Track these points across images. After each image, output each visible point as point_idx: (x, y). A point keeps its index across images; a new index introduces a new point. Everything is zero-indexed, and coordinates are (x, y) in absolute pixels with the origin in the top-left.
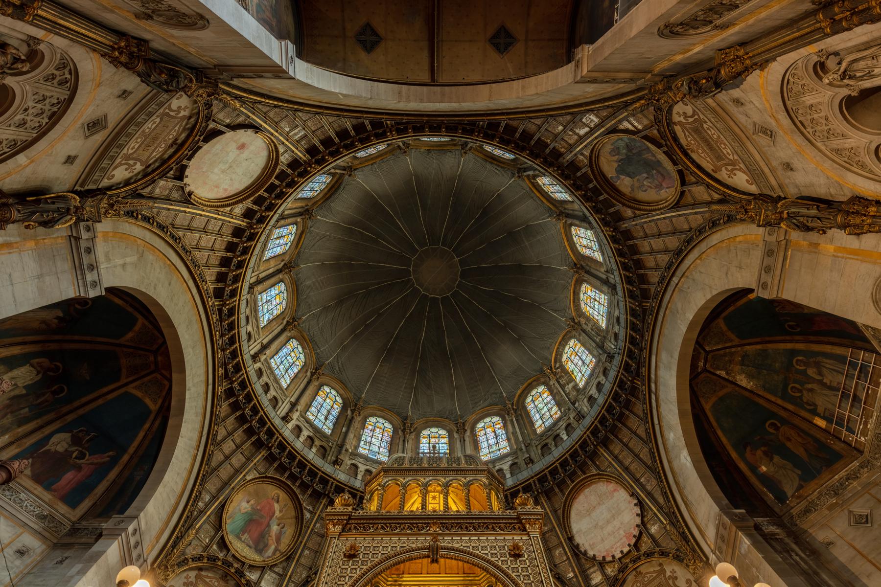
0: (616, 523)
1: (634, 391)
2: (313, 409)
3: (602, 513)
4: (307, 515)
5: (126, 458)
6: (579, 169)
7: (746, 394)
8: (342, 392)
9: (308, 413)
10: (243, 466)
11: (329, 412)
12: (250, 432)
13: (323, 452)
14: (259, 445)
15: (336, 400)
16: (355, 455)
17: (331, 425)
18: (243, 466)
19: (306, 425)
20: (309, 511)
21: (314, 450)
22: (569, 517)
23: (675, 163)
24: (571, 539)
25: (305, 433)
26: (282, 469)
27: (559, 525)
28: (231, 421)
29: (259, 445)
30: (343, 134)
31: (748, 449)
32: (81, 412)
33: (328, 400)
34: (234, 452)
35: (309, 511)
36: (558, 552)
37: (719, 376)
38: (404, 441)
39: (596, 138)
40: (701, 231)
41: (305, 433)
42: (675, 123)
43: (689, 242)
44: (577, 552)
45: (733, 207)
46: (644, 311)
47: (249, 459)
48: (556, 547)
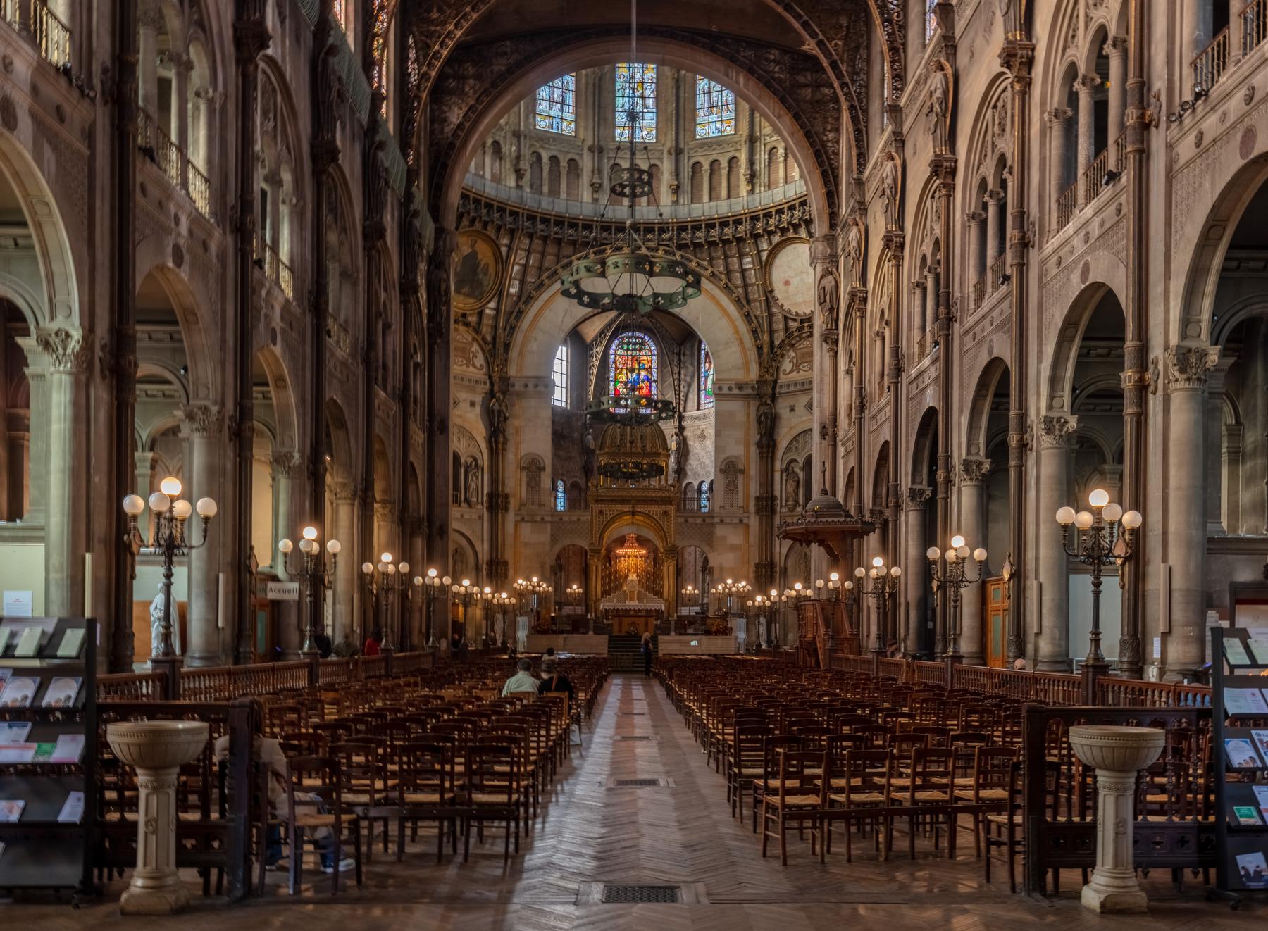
4: (504, 250)
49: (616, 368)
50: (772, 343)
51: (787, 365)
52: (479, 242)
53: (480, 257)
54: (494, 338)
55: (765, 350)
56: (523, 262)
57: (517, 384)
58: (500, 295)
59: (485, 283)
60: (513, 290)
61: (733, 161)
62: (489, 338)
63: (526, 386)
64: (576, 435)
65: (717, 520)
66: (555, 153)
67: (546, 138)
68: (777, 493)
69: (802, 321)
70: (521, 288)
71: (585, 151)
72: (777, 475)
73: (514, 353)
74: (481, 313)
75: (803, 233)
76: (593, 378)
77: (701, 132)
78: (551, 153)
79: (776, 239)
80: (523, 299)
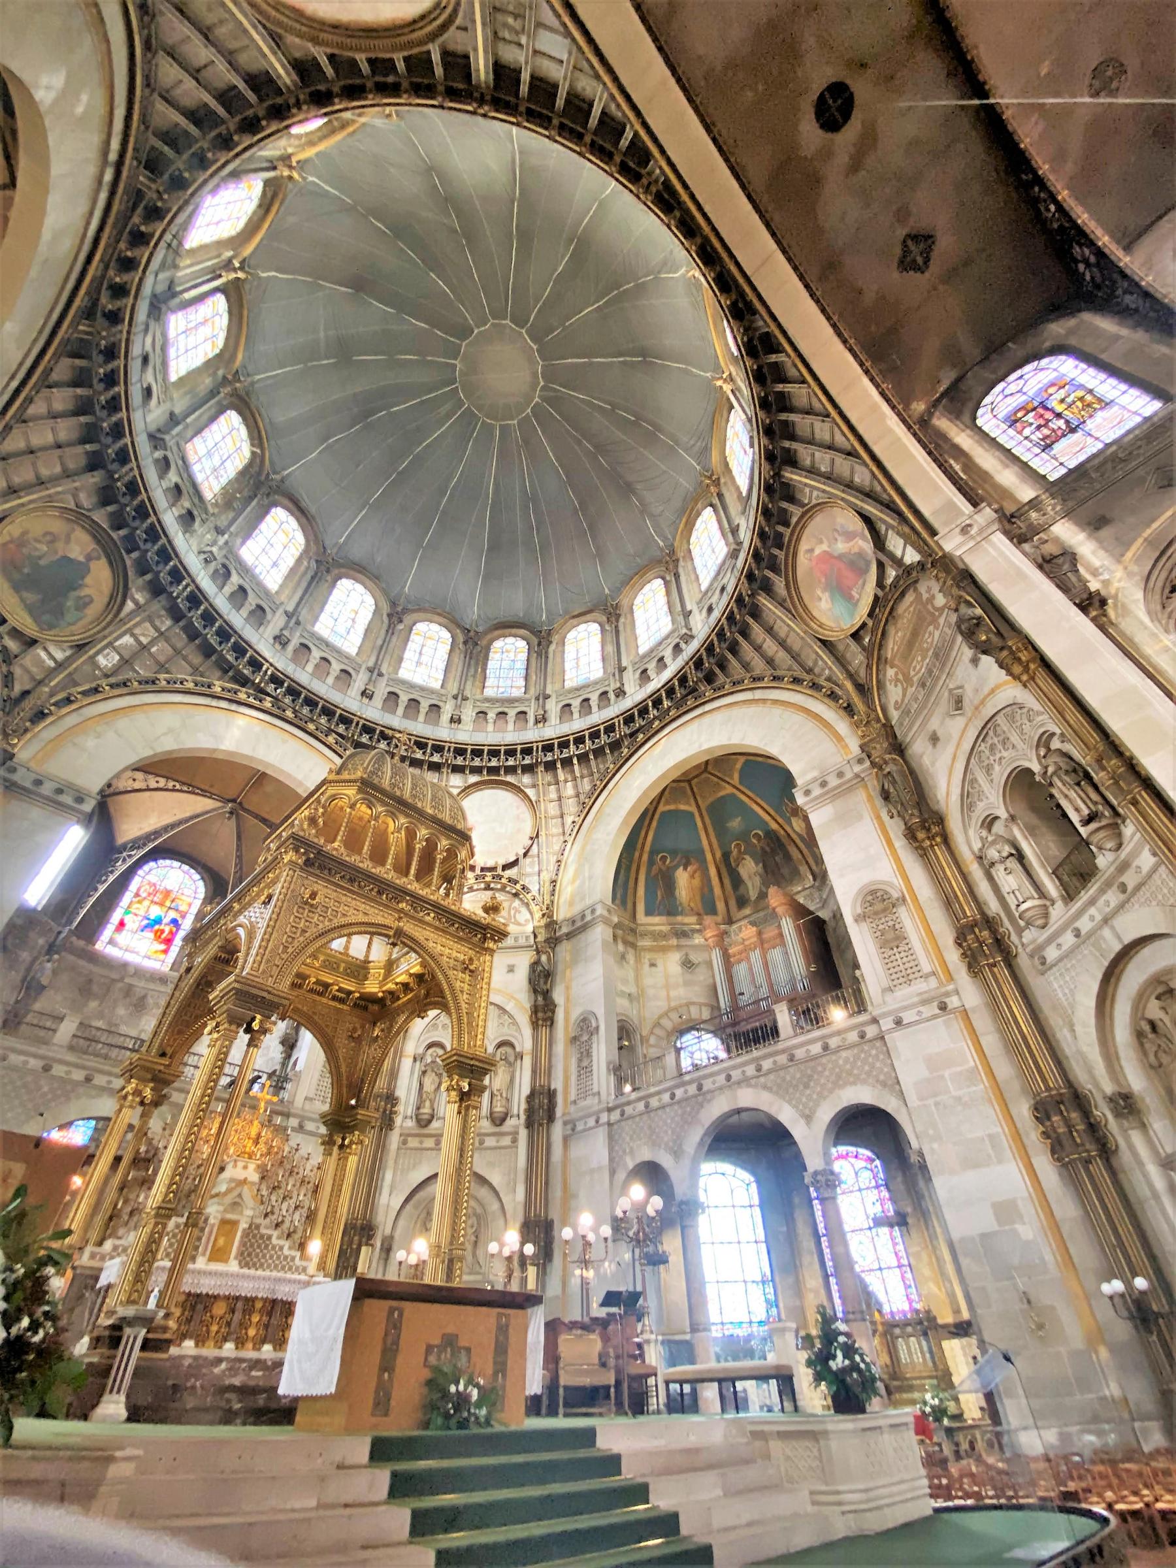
1: (615, 746)
4: (130, 605)
6: (792, 499)
10: (54, 480)
12: (89, 435)
14: (94, 463)
17: (217, 489)
18: (54, 480)
19: (180, 462)
20: (136, 602)
23: (871, 614)
26: (118, 522)
28: (62, 399)
29: (94, 463)
30: (579, 106)
34: (44, 449)
35: (136, 602)
38: (313, 578)
39: (842, 499)
40: (815, 686)
42: (916, 590)
43: (796, 680)
45: (858, 696)
46: (695, 690)
47: (67, 474)
49: (137, 895)
52: (103, 561)
53: (88, 580)
54: (25, 693)
56: (144, 640)
57: (21, 772)
58: (80, 647)
59: (70, 617)
60: (102, 660)
61: (435, 708)
62: (18, 689)
63: (38, 783)
64: (25, 956)
65: (293, 1122)
66: (247, 587)
67: (245, 570)
68: (401, 1092)
69: (482, 869)
70: (116, 671)
71: (281, 611)
72: (406, 1064)
73: (46, 731)
74: (33, 642)
75: (510, 778)
76: (102, 888)
77: (405, 673)
78: (241, 582)
79: (473, 779)
80: (113, 680)
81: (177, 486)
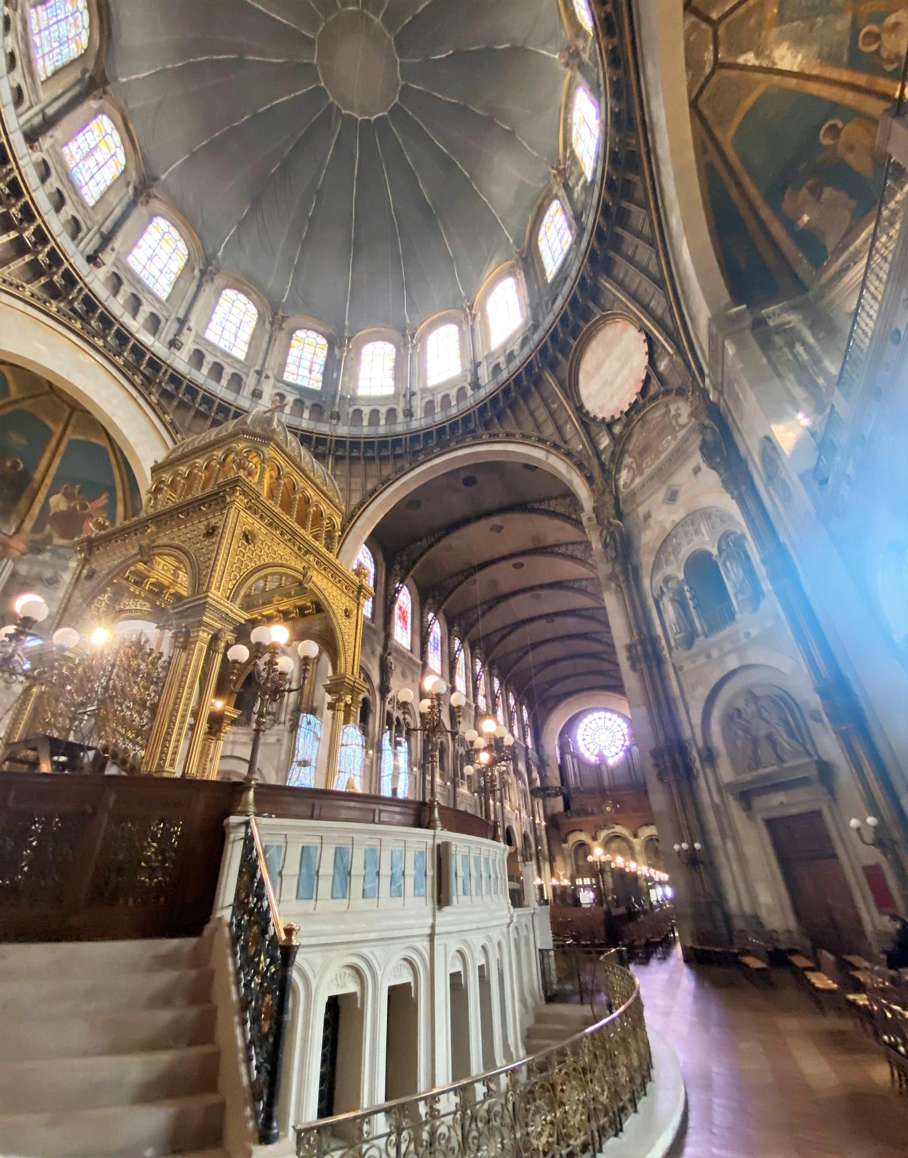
0: (626, 372)
2: (290, 368)
3: (611, 365)
5: (120, 494)
7: (792, 83)
8: (321, 329)
9: (286, 374)
11: (312, 362)
13: (318, 411)
15: (317, 344)
16: (354, 399)
19: (288, 388)
21: (306, 415)
22: (577, 383)
24: (579, 409)
25: (290, 398)
27: (567, 397)
31: (788, 191)
32: (53, 471)
33: (307, 347)
36: (569, 426)
37: (744, 68)
41: (290, 398)
44: (586, 420)
48: (566, 423)
50: (602, 465)
51: (624, 476)
55: (596, 472)
69: (627, 414)
81: (296, 401)
